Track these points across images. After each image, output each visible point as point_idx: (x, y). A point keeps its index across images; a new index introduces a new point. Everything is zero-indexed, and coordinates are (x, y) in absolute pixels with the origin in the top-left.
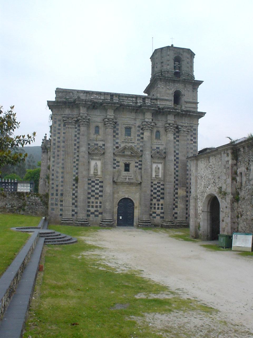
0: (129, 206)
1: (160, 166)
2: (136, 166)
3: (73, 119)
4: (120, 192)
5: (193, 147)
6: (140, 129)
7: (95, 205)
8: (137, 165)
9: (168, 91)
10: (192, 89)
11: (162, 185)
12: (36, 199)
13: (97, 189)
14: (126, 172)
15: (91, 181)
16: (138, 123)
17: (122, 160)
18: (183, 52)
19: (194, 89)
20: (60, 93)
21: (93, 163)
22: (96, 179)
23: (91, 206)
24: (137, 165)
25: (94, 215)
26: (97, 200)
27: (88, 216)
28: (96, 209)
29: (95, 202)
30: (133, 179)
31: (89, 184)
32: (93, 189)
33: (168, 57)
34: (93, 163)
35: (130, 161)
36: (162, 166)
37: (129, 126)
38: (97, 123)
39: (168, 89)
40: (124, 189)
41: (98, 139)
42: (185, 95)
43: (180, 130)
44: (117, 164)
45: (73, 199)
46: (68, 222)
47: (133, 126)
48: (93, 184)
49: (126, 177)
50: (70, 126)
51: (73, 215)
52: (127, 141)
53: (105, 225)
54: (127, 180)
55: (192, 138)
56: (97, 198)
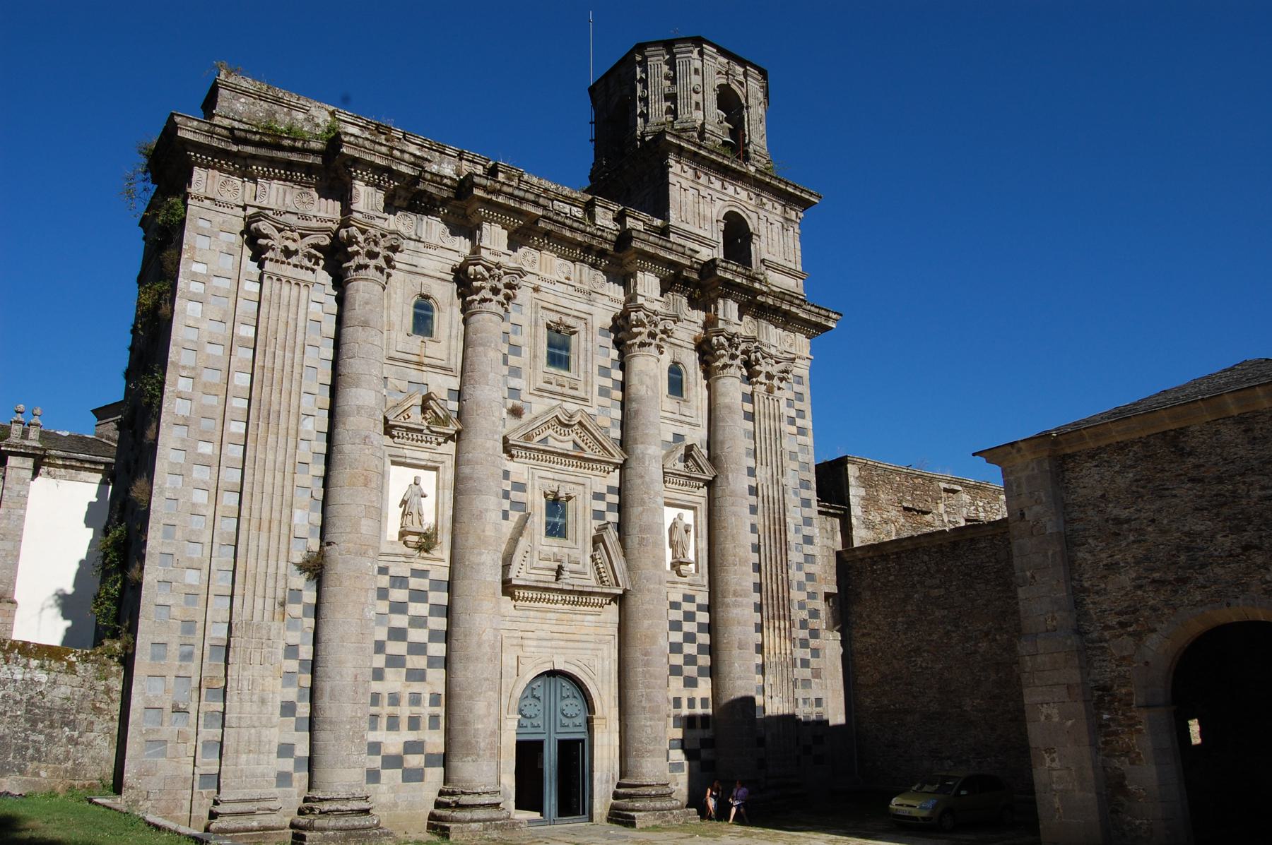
0: (566, 716)
1: (688, 517)
2: (598, 515)
3: (308, 240)
4: (526, 642)
5: (797, 450)
6: (609, 341)
7: (404, 711)
8: (602, 506)
9: (705, 209)
10: (782, 220)
11: (700, 608)
12: (40, 683)
13: (418, 622)
14: (551, 540)
15: (387, 578)
16: (603, 316)
17: (536, 478)
18: (745, 74)
19: (787, 219)
20: (243, 100)
21: (399, 480)
22: (416, 566)
23: (383, 722)
24: (602, 506)
25: (400, 771)
26: (416, 687)
27: (373, 776)
28: (411, 736)
29: (405, 700)
30: (585, 574)
31: (383, 594)
32: (400, 621)
33: (696, 80)
34: (399, 480)
35: (573, 486)
36: (696, 517)
37: (564, 318)
38: (425, 280)
39: (703, 197)
40: (545, 627)
41: (426, 361)
42: (759, 237)
43: (758, 368)
44: (516, 496)
45: (288, 677)
46: (255, 824)
47: (580, 326)
48: (399, 595)
49: (555, 565)
50: (287, 271)
51: (284, 779)
52: (559, 389)
53: (474, 826)
54: (566, 575)
55: (793, 413)
56: (416, 675)
